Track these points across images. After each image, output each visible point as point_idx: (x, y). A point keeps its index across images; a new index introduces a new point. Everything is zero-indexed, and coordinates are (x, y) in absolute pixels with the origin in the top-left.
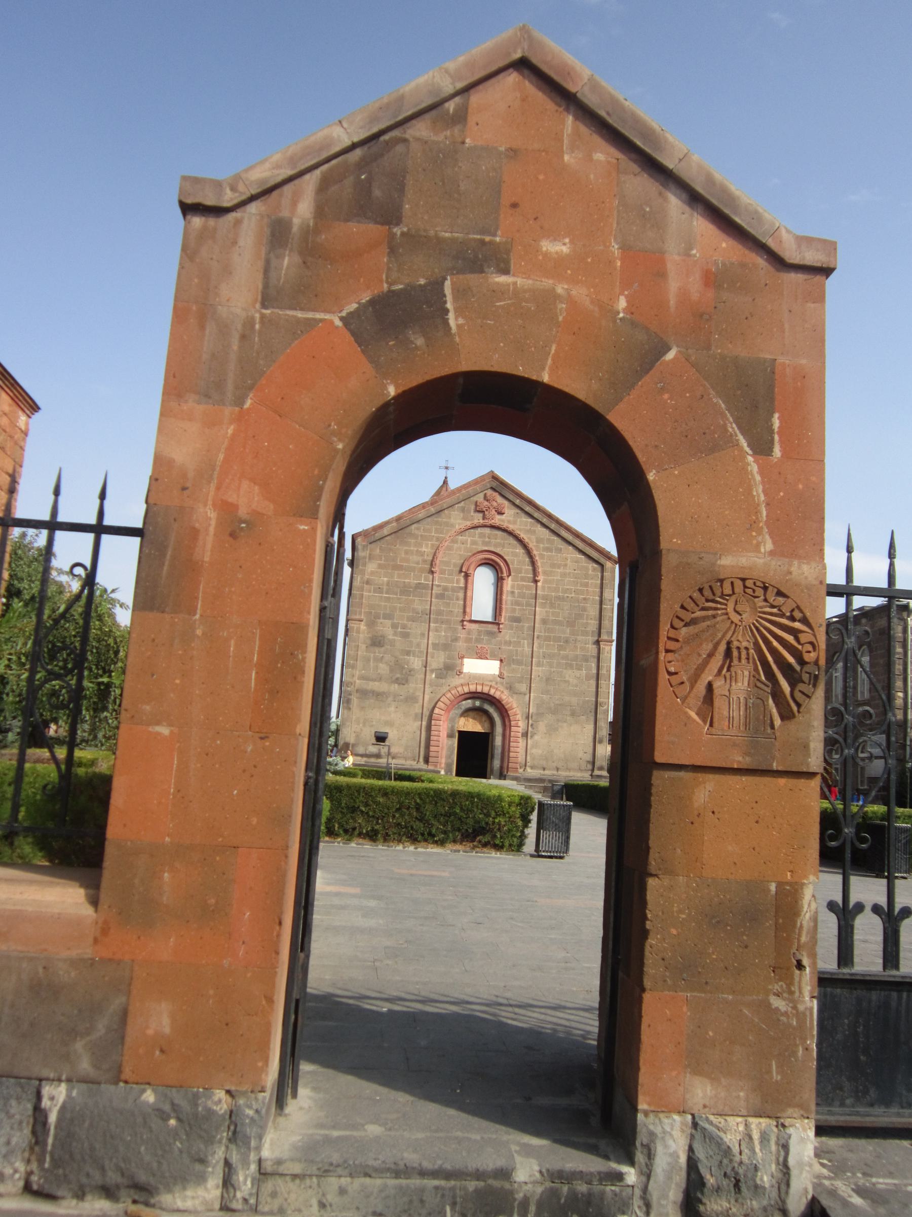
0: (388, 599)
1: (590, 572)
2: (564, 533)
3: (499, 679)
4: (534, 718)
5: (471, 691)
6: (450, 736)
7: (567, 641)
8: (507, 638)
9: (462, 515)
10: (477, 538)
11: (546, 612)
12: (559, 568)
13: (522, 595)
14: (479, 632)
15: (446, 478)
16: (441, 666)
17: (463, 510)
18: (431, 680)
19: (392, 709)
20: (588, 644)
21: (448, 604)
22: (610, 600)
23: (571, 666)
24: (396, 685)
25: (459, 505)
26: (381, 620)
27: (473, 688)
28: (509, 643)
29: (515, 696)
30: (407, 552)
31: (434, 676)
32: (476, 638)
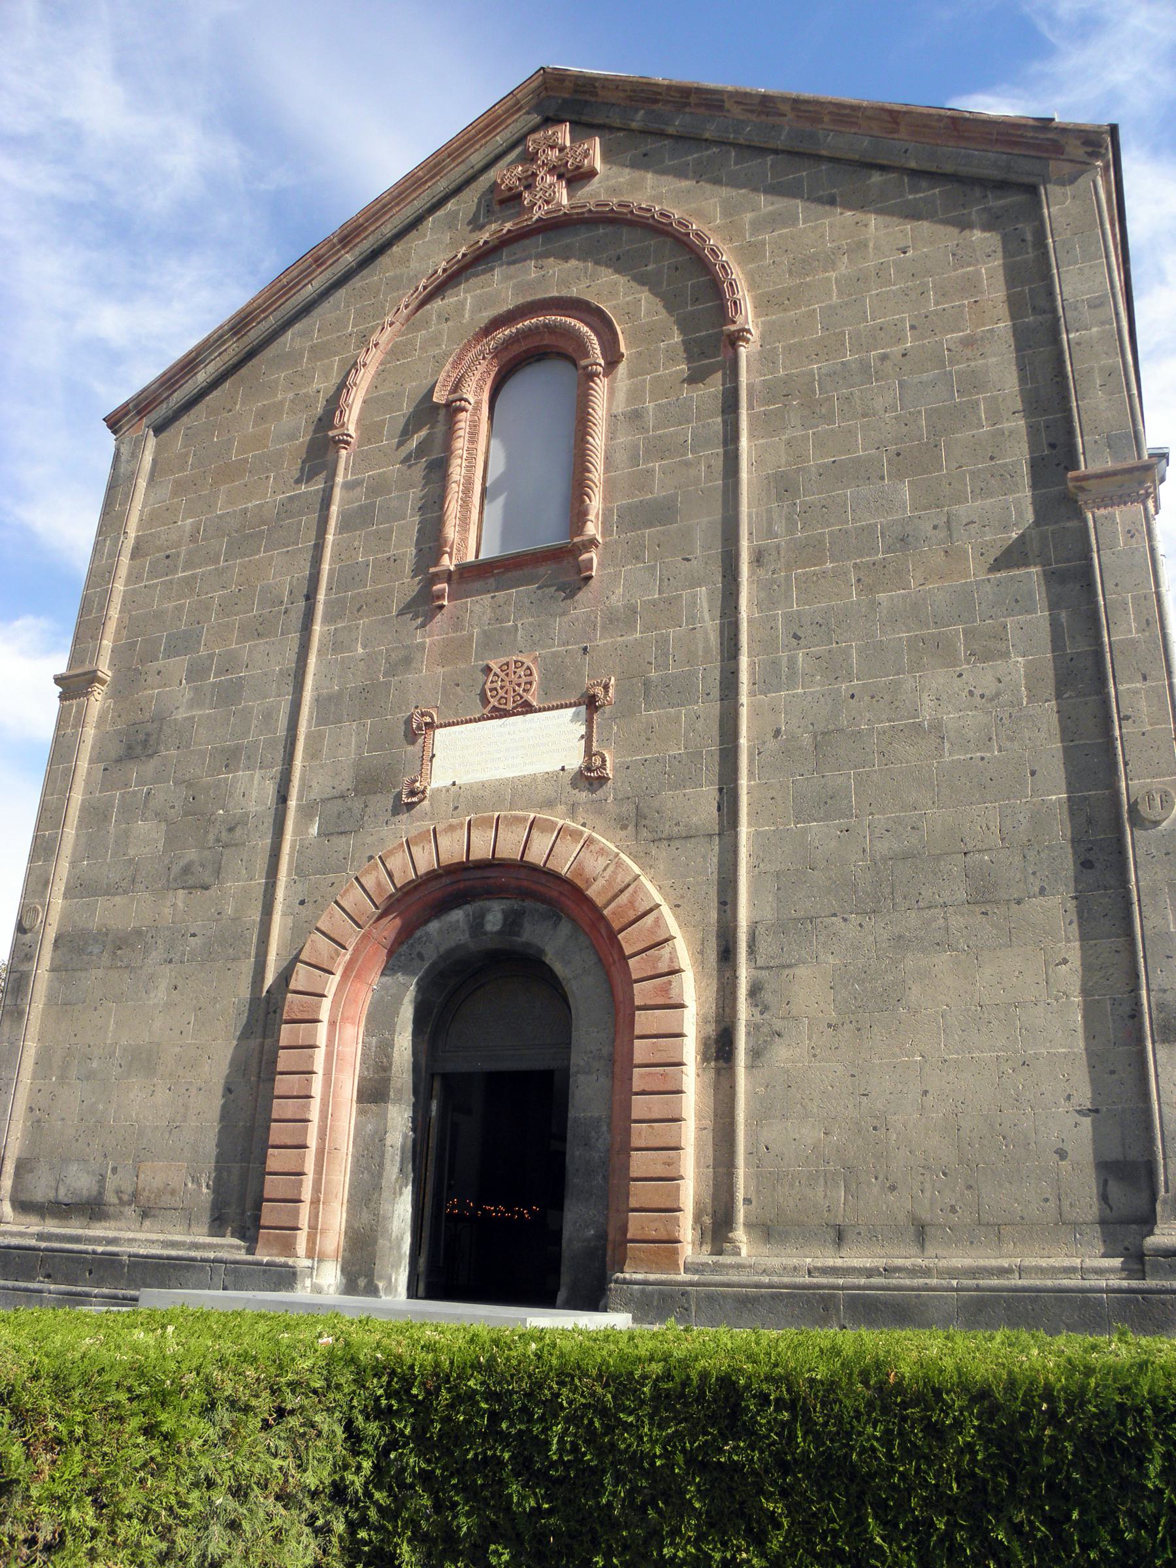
2: (833, 142)
4: (762, 947)
5: (446, 859)
8: (617, 599)
11: (789, 443)
12: (831, 264)
16: (346, 782)
18: (301, 850)
19: (160, 994)
23: (942, 650)
24: (181, 892)
25: (440, 213)
28: (625, 619)
29: (661, 853)
30: (262, 417)
31: (314, 830)
32: (484, 632)
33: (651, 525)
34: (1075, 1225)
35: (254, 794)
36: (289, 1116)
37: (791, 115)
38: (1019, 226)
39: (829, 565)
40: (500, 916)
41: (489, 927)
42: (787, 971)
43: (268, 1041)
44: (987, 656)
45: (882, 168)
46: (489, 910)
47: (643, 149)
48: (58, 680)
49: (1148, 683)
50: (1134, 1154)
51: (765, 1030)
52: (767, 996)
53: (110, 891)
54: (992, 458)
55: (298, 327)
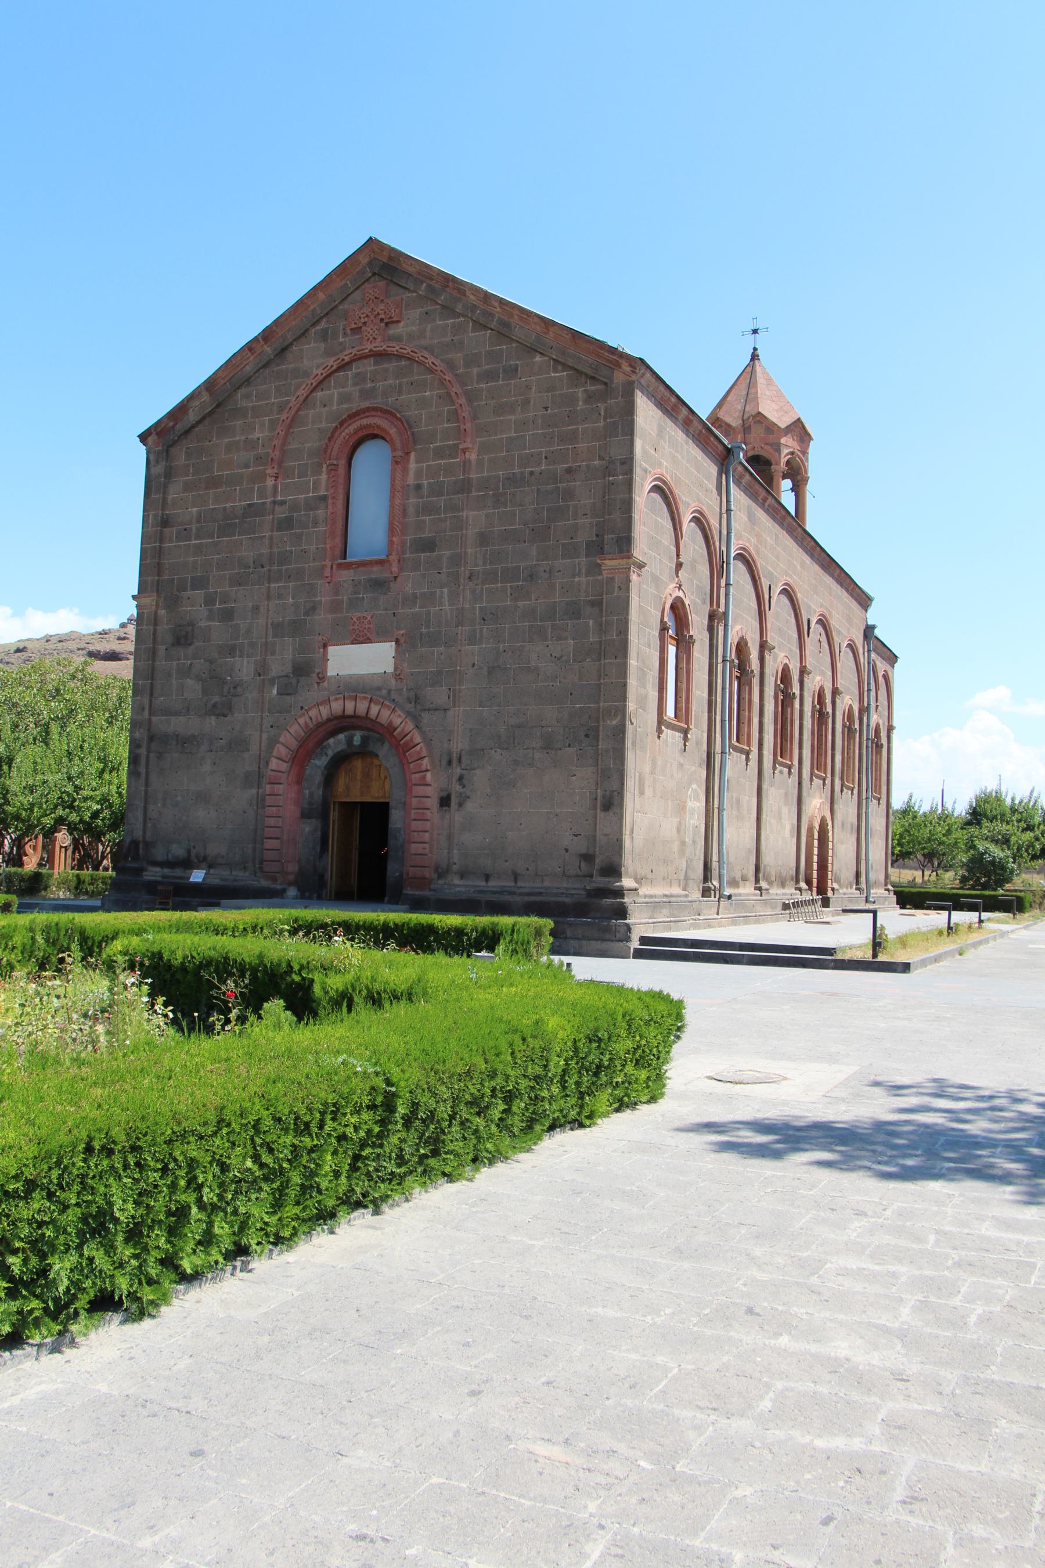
0: (199, 549)
1: (581, 405)
3: (393, 681)
4: (465, 761)
6: (305, 815)
7: (532, 577)
8: (409, 589)
9: (323, 345)
10: (350, 388)
13: (437, 490)
14: (356, 584)
15: (755, 349)
16: (288, 669)
17: (324, 336)
19: (207, 767)
20: (579, 574)
21: (299, 537)
22: (623, 463)
24: (213, 718)
25: (318, 328)
26: (189, 593)
27: (337, 707)
30: (229, 448)
31: (275, 691)
32: (350, 599)
33: (424, 552)
34: (569, 877)
35: (245, 670)
36: (272, 825)
37: (498, 309)
38: (599, 405)
39: (499, 585)
40: (359, 738)
41: (355, 743)
42: (472, 771)
43: (261, 791)
44: (560, 638)
45: (541, 353)
46: (355, 735)
47: (425, 309)
48: (134, 597)
49: (617, 660)
50: (591, 852)
51: (463, 795)
52: (465, 782)
53: (177, 714)
54: (572, 538)
55: (243, 391)
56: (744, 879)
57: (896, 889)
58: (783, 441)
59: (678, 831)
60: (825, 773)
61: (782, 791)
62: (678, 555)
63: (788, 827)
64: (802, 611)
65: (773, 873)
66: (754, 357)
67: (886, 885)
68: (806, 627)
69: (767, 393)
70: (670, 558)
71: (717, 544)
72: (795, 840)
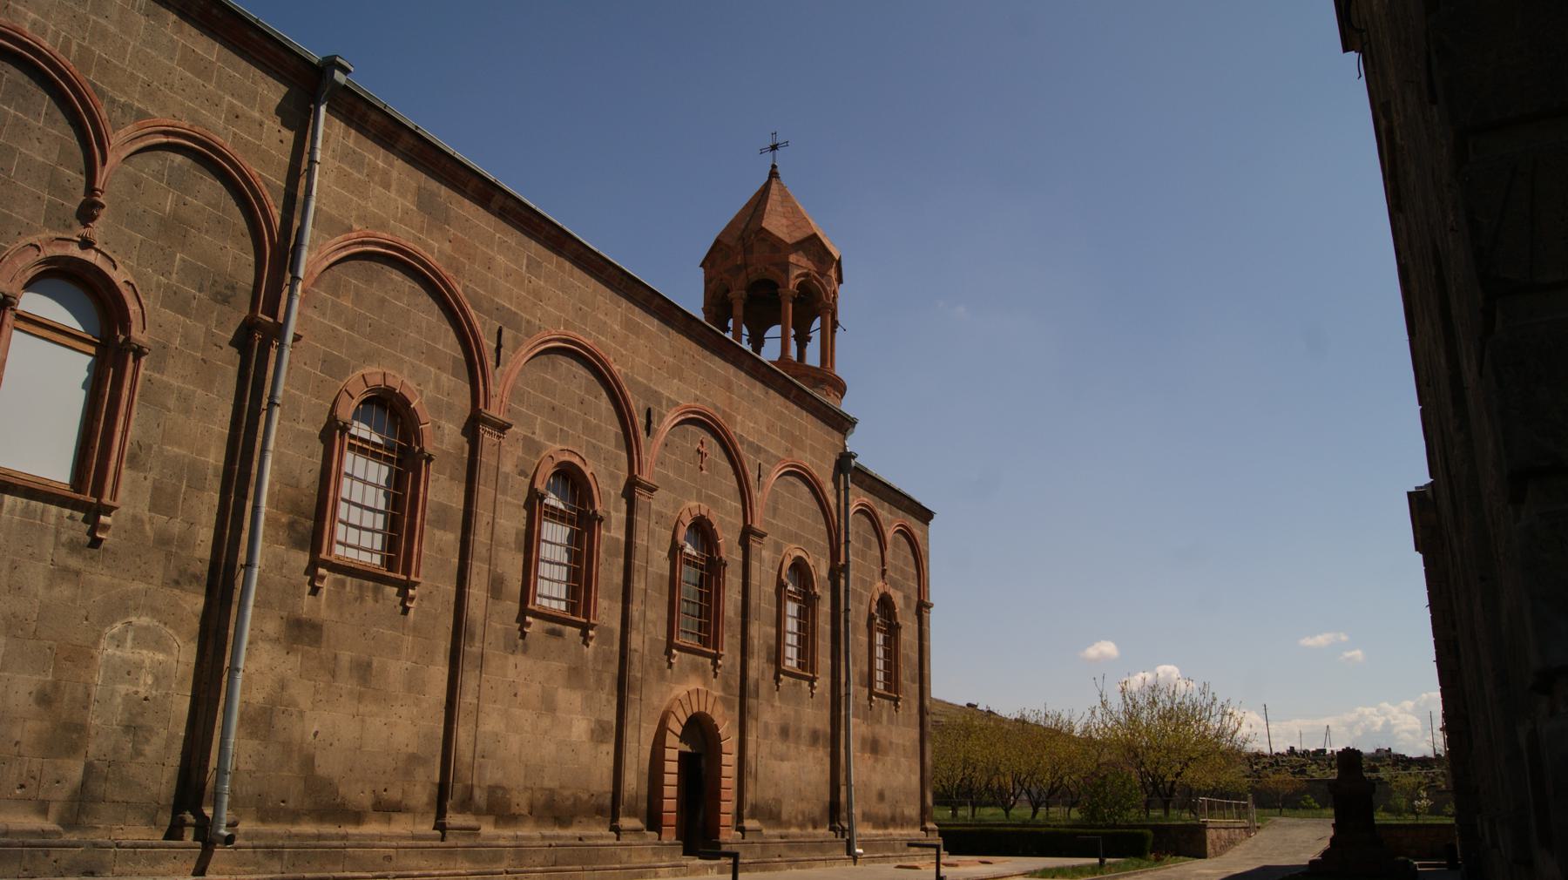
15: (774, 167)
56: (387, 809)
57: (941, 828)
58: (793, 258)
59: (45, 699)
60: (716, 648)
61: (558, 666)
62: (91, 189)
63: (580, 728)
64: (629, 394)
65: (520, 801)
66: (773, 174)
67: (923, 822)
68: (640, 421)
69: (780, 209)
70: (55, 185)
71: (276, 213)
72: (610, 748)
